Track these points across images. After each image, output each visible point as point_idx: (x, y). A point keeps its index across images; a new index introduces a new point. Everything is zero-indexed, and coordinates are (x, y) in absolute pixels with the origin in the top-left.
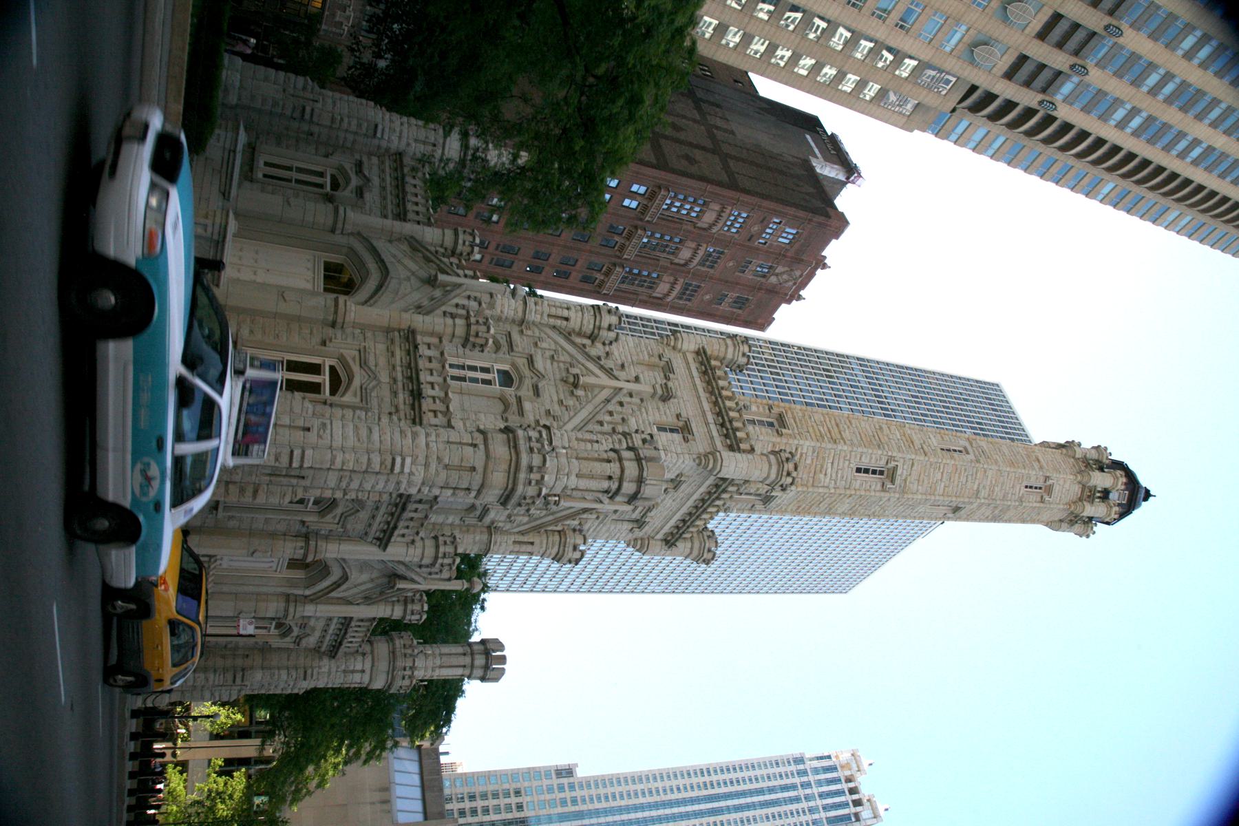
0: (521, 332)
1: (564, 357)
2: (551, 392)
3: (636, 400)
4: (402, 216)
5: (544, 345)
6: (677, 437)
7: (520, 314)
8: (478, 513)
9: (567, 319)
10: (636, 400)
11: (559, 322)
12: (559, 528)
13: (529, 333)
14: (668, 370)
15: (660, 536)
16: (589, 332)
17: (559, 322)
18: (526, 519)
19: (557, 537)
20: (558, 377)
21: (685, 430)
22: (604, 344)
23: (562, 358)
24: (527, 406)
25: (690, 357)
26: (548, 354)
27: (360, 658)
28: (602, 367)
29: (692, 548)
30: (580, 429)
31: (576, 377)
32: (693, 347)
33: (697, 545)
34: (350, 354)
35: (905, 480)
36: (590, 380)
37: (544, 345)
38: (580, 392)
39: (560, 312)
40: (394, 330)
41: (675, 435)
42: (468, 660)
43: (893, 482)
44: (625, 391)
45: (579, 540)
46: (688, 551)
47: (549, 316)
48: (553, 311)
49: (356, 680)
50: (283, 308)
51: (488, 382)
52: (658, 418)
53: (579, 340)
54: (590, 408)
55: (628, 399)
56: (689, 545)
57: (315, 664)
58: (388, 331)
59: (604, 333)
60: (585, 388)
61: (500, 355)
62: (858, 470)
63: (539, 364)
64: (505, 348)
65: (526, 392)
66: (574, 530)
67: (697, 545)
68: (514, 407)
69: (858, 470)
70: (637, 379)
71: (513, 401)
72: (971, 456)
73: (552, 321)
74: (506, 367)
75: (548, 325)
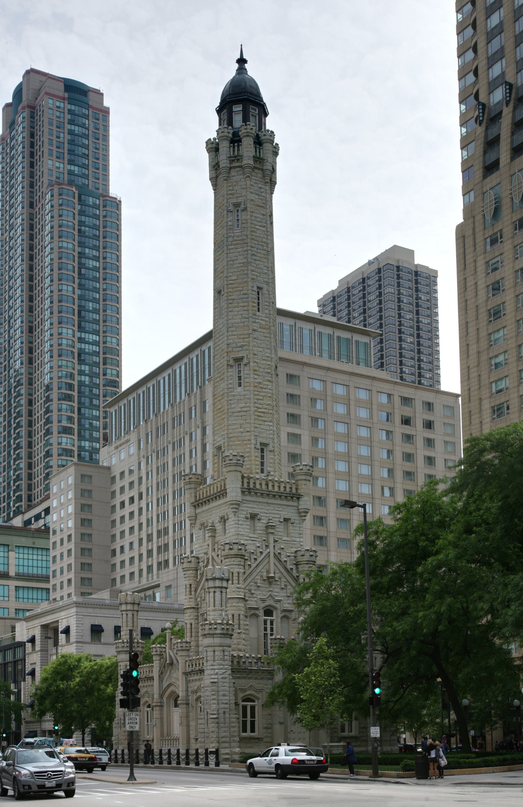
0: (201, 608)
4: (152, 678)
5: (203, 596)
7: (192, 610)
8: (287, 614)
9: (191, 585)
12: (294, 567)
15: (295, 504)
16: (194, 572)
17: (193, 589)
18: (289, 587)
19: (300, 566)
21: (224, 520)
22: (199, 563)
29: (301, 480)
33: (299, 477)
34: (195, 697)
37: (203, 596)
39: (188, 589)
40: (186, 680)
41: (227, 524)
43: (242, 358)
44: (213, 554)
45: (299, 554)
46: (304, 482)
48: (188, 593)
50: (185, 723)
53: (199, 577)
56: (300, 482)
58: (188, 682)
59: (193, 565)
62: (240, 385)
66: (295, 557)
67: (299, 477)
69: (240, 385)
70: (208, 545)
73: (193, 593)
75: (195, 595)
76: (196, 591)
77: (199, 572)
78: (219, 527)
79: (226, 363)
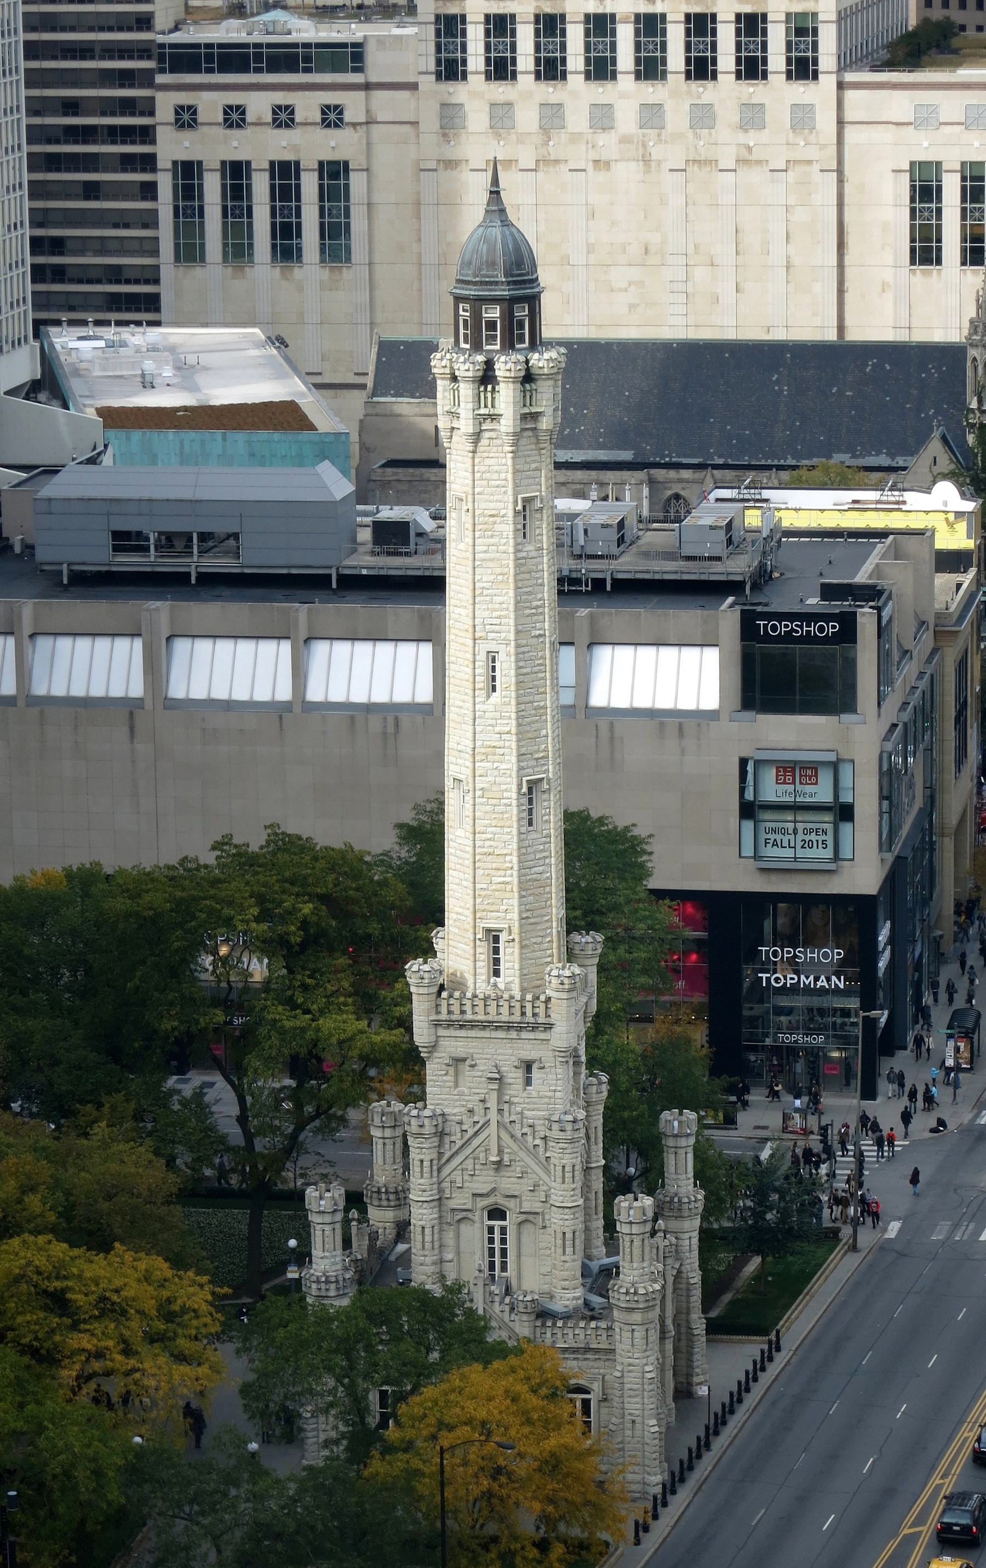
1: (469, 1164)
2: (508, 1183)
3: (506, 1107)
5: (459, 1179)
6: (536, 1074)
10: (506, 1107)
11: (435, 1168)
13: (447, 1191)
14: (458, 1061)
17: (435, 1168)
20: (491, 1173)
23: (470, 1167)
24: (526, 1207)
25: (441, 1032)
26: (466, 1177)
27: (681, 1242)
28: (476, 1134)
30: (548, 1172)
31: (494, 1163)
32: (432, 1030)
35: (537, 759)
36: (494, 1149)
38: (506, 1158)
42: (682, 1151)
47: (432, 1176)
49: (695, 1241)
51: (503, 1230)
52: (520, 1087)
54: (523, 1154)
55: (506, 1114)
57: (684, 1275)
60: (500, 1152)
61: (476, 1218)
62: (530, 824)
63: (484, 1189)
64: (470, 1215)
65: (511, 1204)
68: (531, 1217)
69: (530, 824)
71: (523, 1217)
72: (502, 649)
74: (486, 1214)
76: (439, 1170)
77: (447, 1140)
78: (515, 1077)
79: (514, 788)
